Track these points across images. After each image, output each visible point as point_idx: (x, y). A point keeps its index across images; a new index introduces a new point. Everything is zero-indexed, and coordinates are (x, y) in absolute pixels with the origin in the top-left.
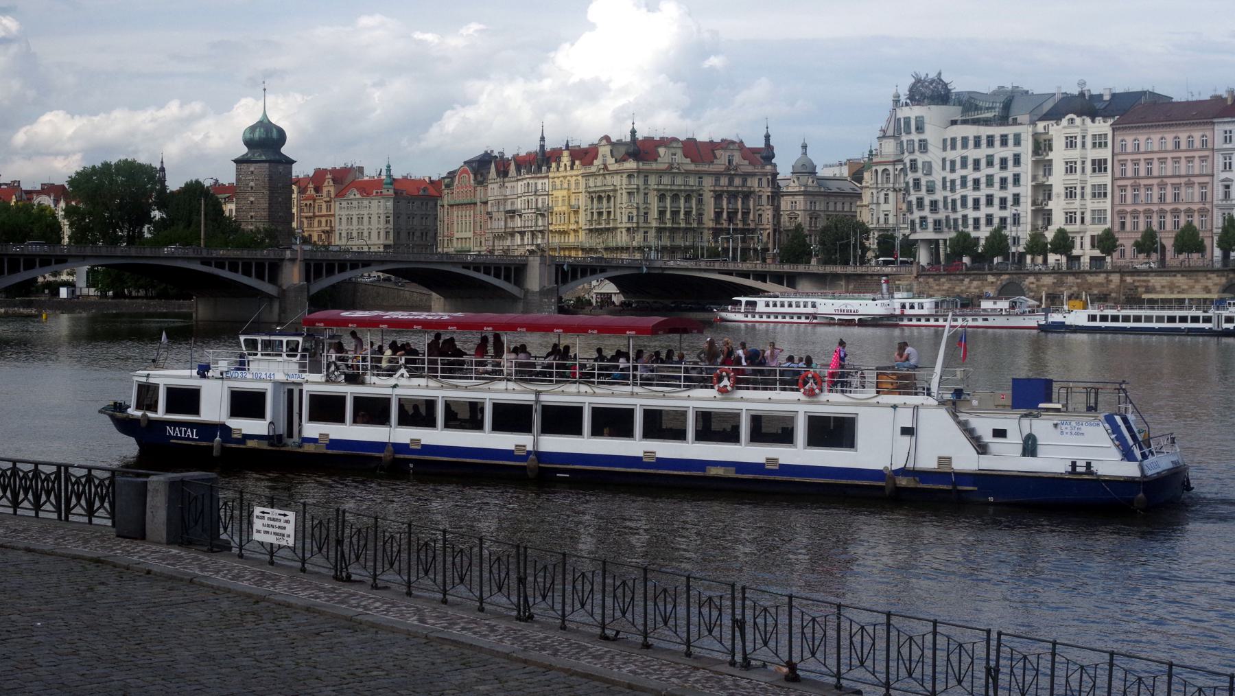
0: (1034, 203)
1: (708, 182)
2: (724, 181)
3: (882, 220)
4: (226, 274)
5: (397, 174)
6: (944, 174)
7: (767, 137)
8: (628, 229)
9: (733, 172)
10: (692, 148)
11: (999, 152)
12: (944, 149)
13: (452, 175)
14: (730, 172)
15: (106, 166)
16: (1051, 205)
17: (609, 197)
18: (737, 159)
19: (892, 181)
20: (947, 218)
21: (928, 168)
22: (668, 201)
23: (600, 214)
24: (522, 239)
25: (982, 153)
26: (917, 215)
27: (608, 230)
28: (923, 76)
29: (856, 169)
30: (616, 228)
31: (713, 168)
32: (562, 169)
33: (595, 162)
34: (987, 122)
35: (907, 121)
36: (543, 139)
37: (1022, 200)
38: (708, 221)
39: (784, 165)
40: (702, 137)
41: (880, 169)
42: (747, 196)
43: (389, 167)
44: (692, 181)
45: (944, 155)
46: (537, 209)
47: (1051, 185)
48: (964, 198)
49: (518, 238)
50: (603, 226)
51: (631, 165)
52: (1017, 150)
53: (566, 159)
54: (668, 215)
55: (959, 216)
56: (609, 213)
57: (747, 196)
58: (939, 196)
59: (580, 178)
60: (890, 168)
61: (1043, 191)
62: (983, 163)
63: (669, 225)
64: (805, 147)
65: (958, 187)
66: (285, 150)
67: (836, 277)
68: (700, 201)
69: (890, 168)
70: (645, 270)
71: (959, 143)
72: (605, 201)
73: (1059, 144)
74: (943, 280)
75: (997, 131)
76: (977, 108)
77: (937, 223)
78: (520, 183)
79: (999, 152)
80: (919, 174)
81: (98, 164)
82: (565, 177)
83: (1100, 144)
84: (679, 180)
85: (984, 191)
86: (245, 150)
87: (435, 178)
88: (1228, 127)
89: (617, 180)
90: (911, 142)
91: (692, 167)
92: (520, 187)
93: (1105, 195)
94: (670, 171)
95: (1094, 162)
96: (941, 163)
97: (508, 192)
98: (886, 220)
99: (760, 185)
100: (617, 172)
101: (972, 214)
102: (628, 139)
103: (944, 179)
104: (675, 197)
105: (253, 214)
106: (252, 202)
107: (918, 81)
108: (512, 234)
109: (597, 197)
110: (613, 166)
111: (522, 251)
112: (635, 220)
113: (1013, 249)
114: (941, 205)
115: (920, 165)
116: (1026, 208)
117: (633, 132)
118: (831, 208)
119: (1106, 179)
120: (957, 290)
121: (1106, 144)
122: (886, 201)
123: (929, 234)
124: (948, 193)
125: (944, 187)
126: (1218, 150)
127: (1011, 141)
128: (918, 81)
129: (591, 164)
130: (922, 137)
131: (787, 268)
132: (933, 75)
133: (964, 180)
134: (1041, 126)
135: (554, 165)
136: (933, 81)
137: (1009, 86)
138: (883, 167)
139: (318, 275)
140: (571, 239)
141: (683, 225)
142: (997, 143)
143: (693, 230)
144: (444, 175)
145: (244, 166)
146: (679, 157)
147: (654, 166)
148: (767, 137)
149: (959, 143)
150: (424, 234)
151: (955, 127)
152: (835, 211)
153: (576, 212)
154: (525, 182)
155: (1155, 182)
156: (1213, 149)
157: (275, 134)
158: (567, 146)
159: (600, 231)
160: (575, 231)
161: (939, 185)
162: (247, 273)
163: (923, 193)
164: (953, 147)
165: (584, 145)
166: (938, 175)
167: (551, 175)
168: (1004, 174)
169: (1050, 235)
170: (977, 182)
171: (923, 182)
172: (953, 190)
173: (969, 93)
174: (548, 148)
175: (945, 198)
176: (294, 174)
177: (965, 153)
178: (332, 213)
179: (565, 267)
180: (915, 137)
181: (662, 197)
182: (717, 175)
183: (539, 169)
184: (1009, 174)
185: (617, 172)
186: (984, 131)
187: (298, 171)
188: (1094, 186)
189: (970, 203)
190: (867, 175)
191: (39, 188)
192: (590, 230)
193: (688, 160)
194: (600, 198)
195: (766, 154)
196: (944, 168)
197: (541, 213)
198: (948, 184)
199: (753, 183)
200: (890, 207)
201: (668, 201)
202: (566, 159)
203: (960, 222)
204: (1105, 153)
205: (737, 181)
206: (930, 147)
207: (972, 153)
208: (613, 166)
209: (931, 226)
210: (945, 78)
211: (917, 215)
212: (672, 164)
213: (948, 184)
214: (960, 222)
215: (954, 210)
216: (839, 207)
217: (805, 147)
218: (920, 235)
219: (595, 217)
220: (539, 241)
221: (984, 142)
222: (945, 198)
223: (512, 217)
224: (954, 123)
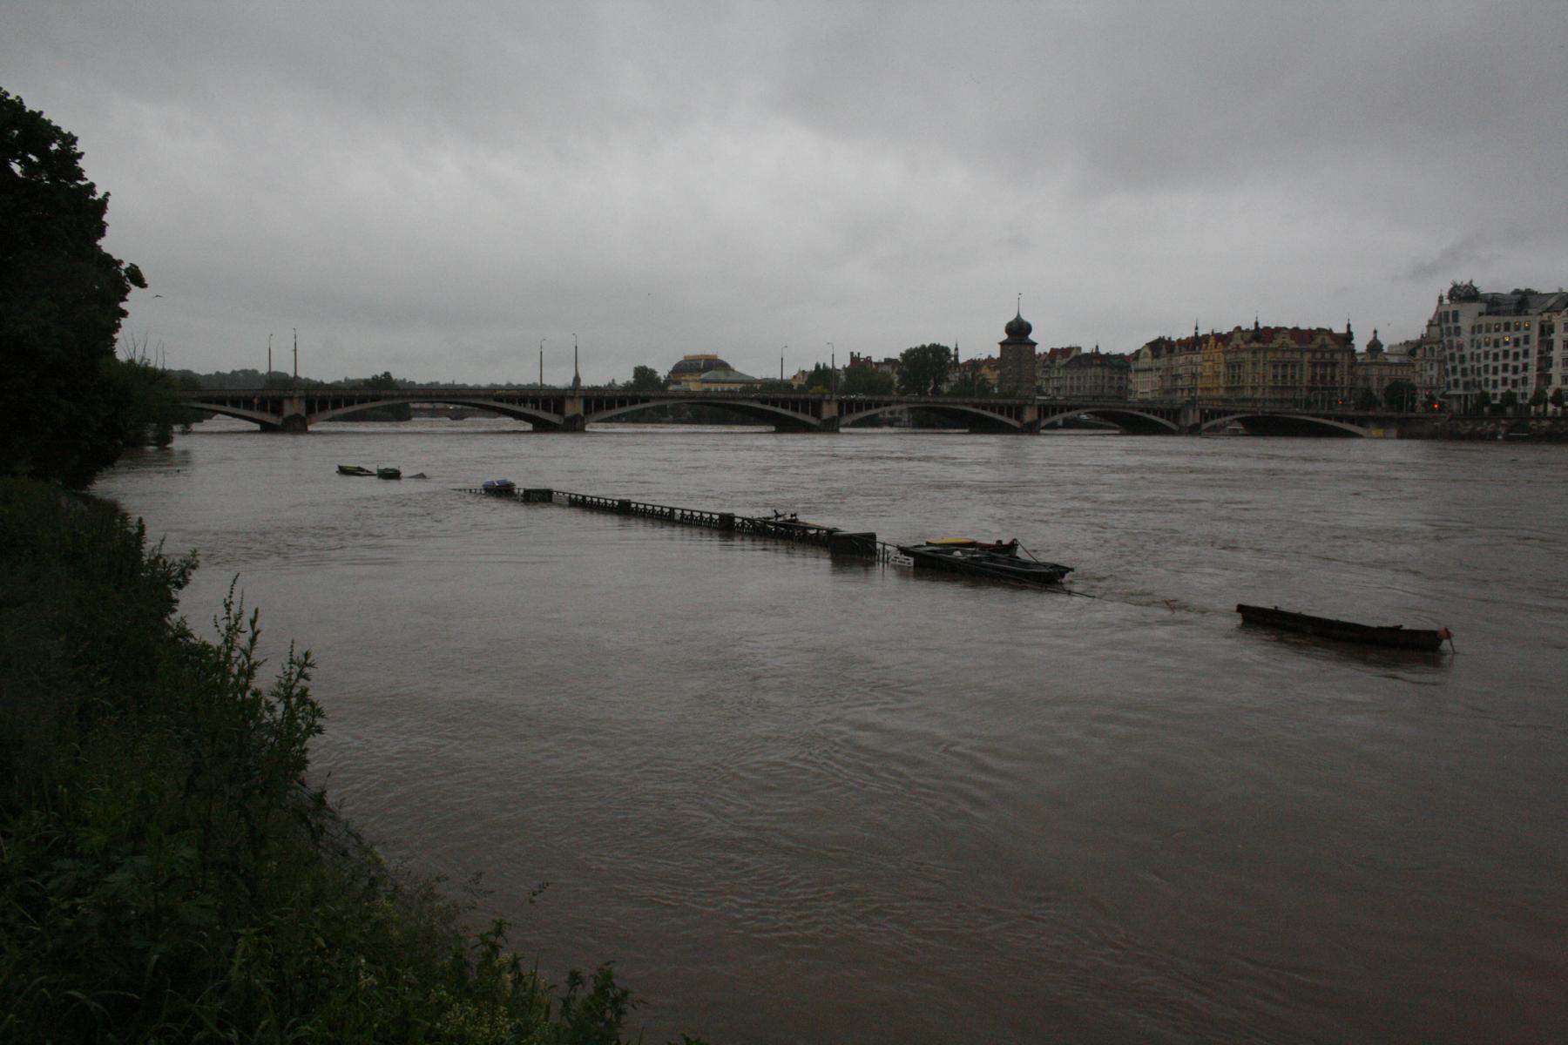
0: (1539, 369)
1: (1307, 356)
2: (1319, 355)
3: (1428, 382)
4: (988, 413)
5: (1103, 351)
6: (1472, 350)
7: (1349, 326)
8: (1252, 387)
9: (1324, 350)
10: (1296, 333)
12: (1473, 332)
13: (1138, 352)
14: (1323, 348)
15: (923, 347)
16: (1552, 371)
17: (1240, 366)
18: (1328, 340)
19: (1436, 354)
20: (1474, 379)
21: (1460, 347)
22: (1280, 368)
23: (1233, 377)
24: (1182, 393)
26: (1451, 378)
27: (1238, 387)
28: (1459, 283)
29: (1413, 346)
30: (1243, 387)
31: (1311, 346)
32: (1209, 348)
33: (1231, 344)
34: (1505, 313)
36: (1197, 328)
37: (1530, 367)
38: (1305, 383)
39: (1360, 344)
40: (1303, 327)
41: (1427, 347)
42: (1334, 365)
44: (1297, 356)
45: (1473, 336)
46: (1193, 374)
47: (1551, 358)
48: (1486, 367)
49: (1180, 392)
50: (1235, 385)
51: (1255, 345)
53: (1212, 342)
54: (1280, 378)
55: (1482, 378)
56: (1239, 377)
57: (1334, 365)
58: (1467, 365)
59: (1221, 354)
60: (1435, 347)
61: (1545, 362)
63: (1280, 385)
64: (1375, 332)
65: (1482, 359)
66: (1032, 337)
67: (1391, 419)
68: (1301, 369)
69: (1435, 347)
70: (1260, 414)
71: (1484, 329)
72: (1237, 369)
73: (1556, 329)
74: (1468, 422)
75: (1513, 320)
76: (1498, 304)
77: (1466, 385)
78: (1181, 358)
80: (1455, 350)
81: (918, 345)
82: (1211, 353)
84: (1288, 355)
85: (1501, 362)
86: (1005, 337)
87: (1127, 353)
89: (1244, 355)
90: (1448, 329)
91: (1297, 346)
92: (1181, 359)
94: (1281, 348)
96: (1469, 341)
97: (1174, 362)
98: (1431, 382)
99: (1343, 359)
100: (1245, 350)
101: (1491, 377)
102: (1253, 328)
103: (1472, 354)
104: (1284, 366)
108: (1176, 390)
109: (1231, 366)
110: (1243, 346)
111: (1183, 401)
112: (1257, 381)
113: (1521, 402)
114: (1469, 372)
115: (1455, 345)
116: (1532, 373)
117: (1257, 324)
118: (1394, 373)
120: (1479, 429)
122: (1432, 368)
123: (1460, 391)
124: (1475, 363)
125: (1472, 359)
129: (1228, 344)
130: (1459, 324)
131: (1361, 414)
132: (1466, 282)
133: (1486, 355)
134: (1546, 316)
135: (1204, 345)
136: (1466, 286)
137: (1523, 288)
138: (1430, 346)
139: (1046, 415)
140: (1214, 394)
141: (1289, 384)
143: (1295, 388)
144: (1133, 352)
146: (1288, 340)
147: (1271, 345)
148: (1349, 326)
149: (1484, 329)
150: (1120, 388)
151: (1481, 317)
152: (1396, 375)
153: (1218, 376)
154: (1184, 357)
158: (1213, 332)
159: (1234, 389)
160: (1217, 388)
161: (1468, 357)
162: (1001, 413)
163: (1457, 362)
164: (1480, 332)
165: (1224, 332)
166: (1467, 351)
167: (1202, 352)
168: (1516, 350)
169: (1550, 393)
170: (1496, 357)
171: (1457, 355)
172: (1478, 361)
173: (1492, 294)
174: (1200, 334)
175: (1473, 367)
176: (1037, 353)
177: (1488, 335)
178: (1061, 375)
179: (1207, 411)
180: (1452, 325)
181: (1275, 367)
182: (1314, 352)
183: (1194, 349)
184: (1520, 350)
185: (1245, 350)
186: (1503, 320)
187: (1039, 350)
189: (1491, 370)
190: (1419, 352)
191: (883, 361)
192: (1227, 389)
193: (1293, 342)
194: (1234, 367)
195: (1348, 337)
196: (1472, 346)
197: (1194, 376)
198: (1475, 357)
199: (1338, 356)
200: (1434, 373)
201: (1280, 368)
202: (1212, 342)
203: (1483, 383)
205: (1327, 356)
206: (1462, 332)
207: (1494, 336)
208: (1243, 346)
209: (1461, 386)
210: (1475, 284)
211: (1451, 378)
212: (1281, 345)
213: (1475, 357)
214: (1483, 383)
215: (1479, 374)
216: (1399, 374)
217: (1375, 332)
218: (1454, 392)
219: (1230, 378)
220: (1193, 395)
222: (1473, 367)
223: (1176, 379)
224: (1481, 314)
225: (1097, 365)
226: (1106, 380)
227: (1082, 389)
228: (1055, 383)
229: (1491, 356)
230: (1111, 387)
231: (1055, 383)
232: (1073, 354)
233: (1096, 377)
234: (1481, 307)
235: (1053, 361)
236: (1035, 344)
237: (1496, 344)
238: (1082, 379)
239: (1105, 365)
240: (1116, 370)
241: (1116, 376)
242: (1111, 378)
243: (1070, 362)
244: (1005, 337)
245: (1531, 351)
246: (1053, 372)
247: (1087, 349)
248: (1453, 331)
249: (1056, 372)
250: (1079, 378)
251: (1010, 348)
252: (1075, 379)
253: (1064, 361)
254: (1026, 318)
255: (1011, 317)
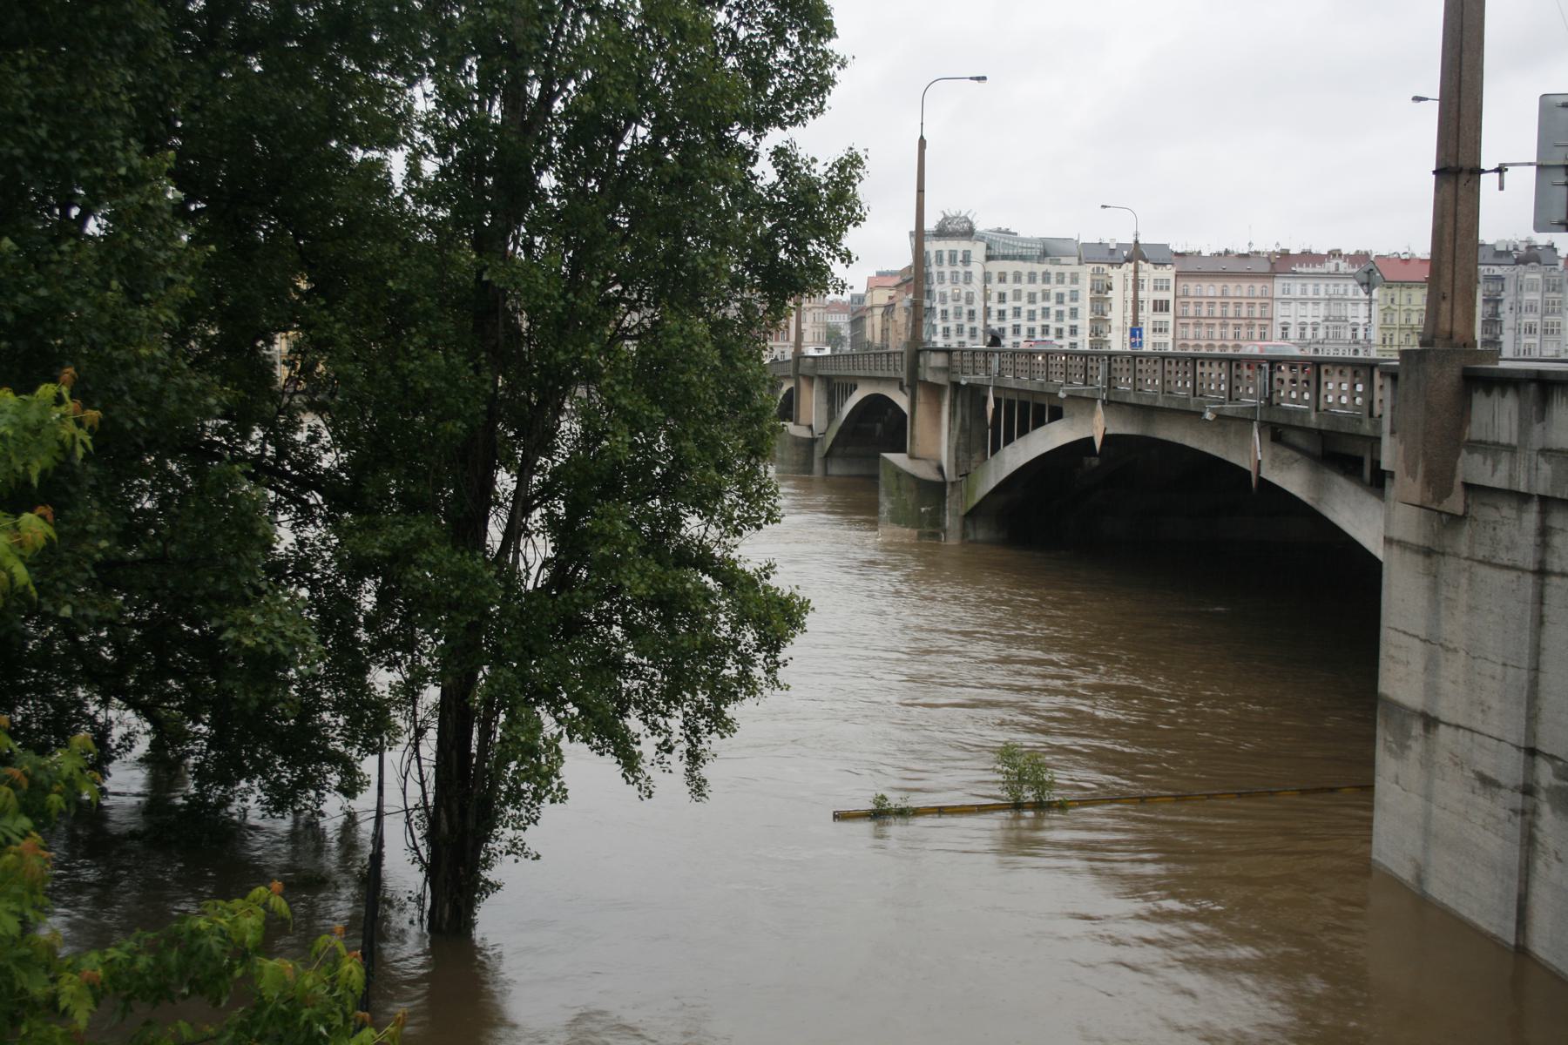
11: (1055, 288)
25: (1038, 287)
35: (939, 254)
37: (1079, 331)
52: (1074, 287)
62: (1039, 296)
73: (1117, 284)
75: (1039, 268)
79: (1055, 288)
83: (1161, 288)
88: (1287, 281)
93: (1166, 330)
95: (1155, 302)
107: (946, 218)
119: (1169, 317)
121: (1168, 288)
126: (1278, 299)
127: (1067, 280)
128: (946, 218)
130: (968, 269)
142: (1053, 280)
155: (1217, 322)
156: (1272, 298)
168: (1060, 308)
177: (1017, 286)
180: (960, 268)
184: (1066, 308)
188: (1155, 322)
204: (1169, 295)
206: (974, 280)
207: (1026, 287)
221: (1039, 279)
229: (1024, 314)
234: (978, 251)
237: (1032, 298)
245: (1079, 316)
248: (961, 277)
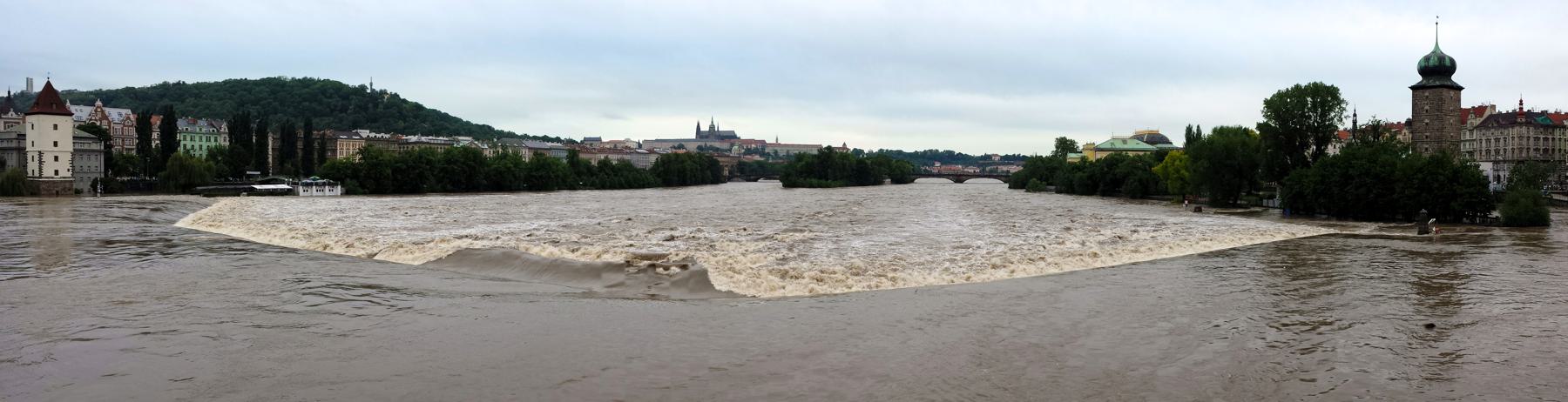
5: (1525, 110)
43: (1521, 101)
86: (1418, 79)
105: (1428, 134)
106: (1427, 124)
145: (1419, 93)
157: (1448, 63)
178: (1474, 138)
225: (1521, 124)
226: (1532, 139)
227: (1502, 152)
228: (1467, 146)
230: (1537, 150)
231: (1467, 146)
232: (1487, 113)
233: (1521, 138)
235: (1464, 122)
236: (1462, 88)
238: (1502, 141)
239: (1530, 123)
240: (1542, 130)
241: (1542, 136)
242: (1537, 139)
243: (1483, 122)
244: (1418, 79)
246: (1465, 134)
247: (1506, 105)
249: (1468, 133)
250: (1497, 140)
251: (1427, 94)
252: (1493, 141)
253: (1478, 121)
254: (1447, 51)
255: (1428, 51)
